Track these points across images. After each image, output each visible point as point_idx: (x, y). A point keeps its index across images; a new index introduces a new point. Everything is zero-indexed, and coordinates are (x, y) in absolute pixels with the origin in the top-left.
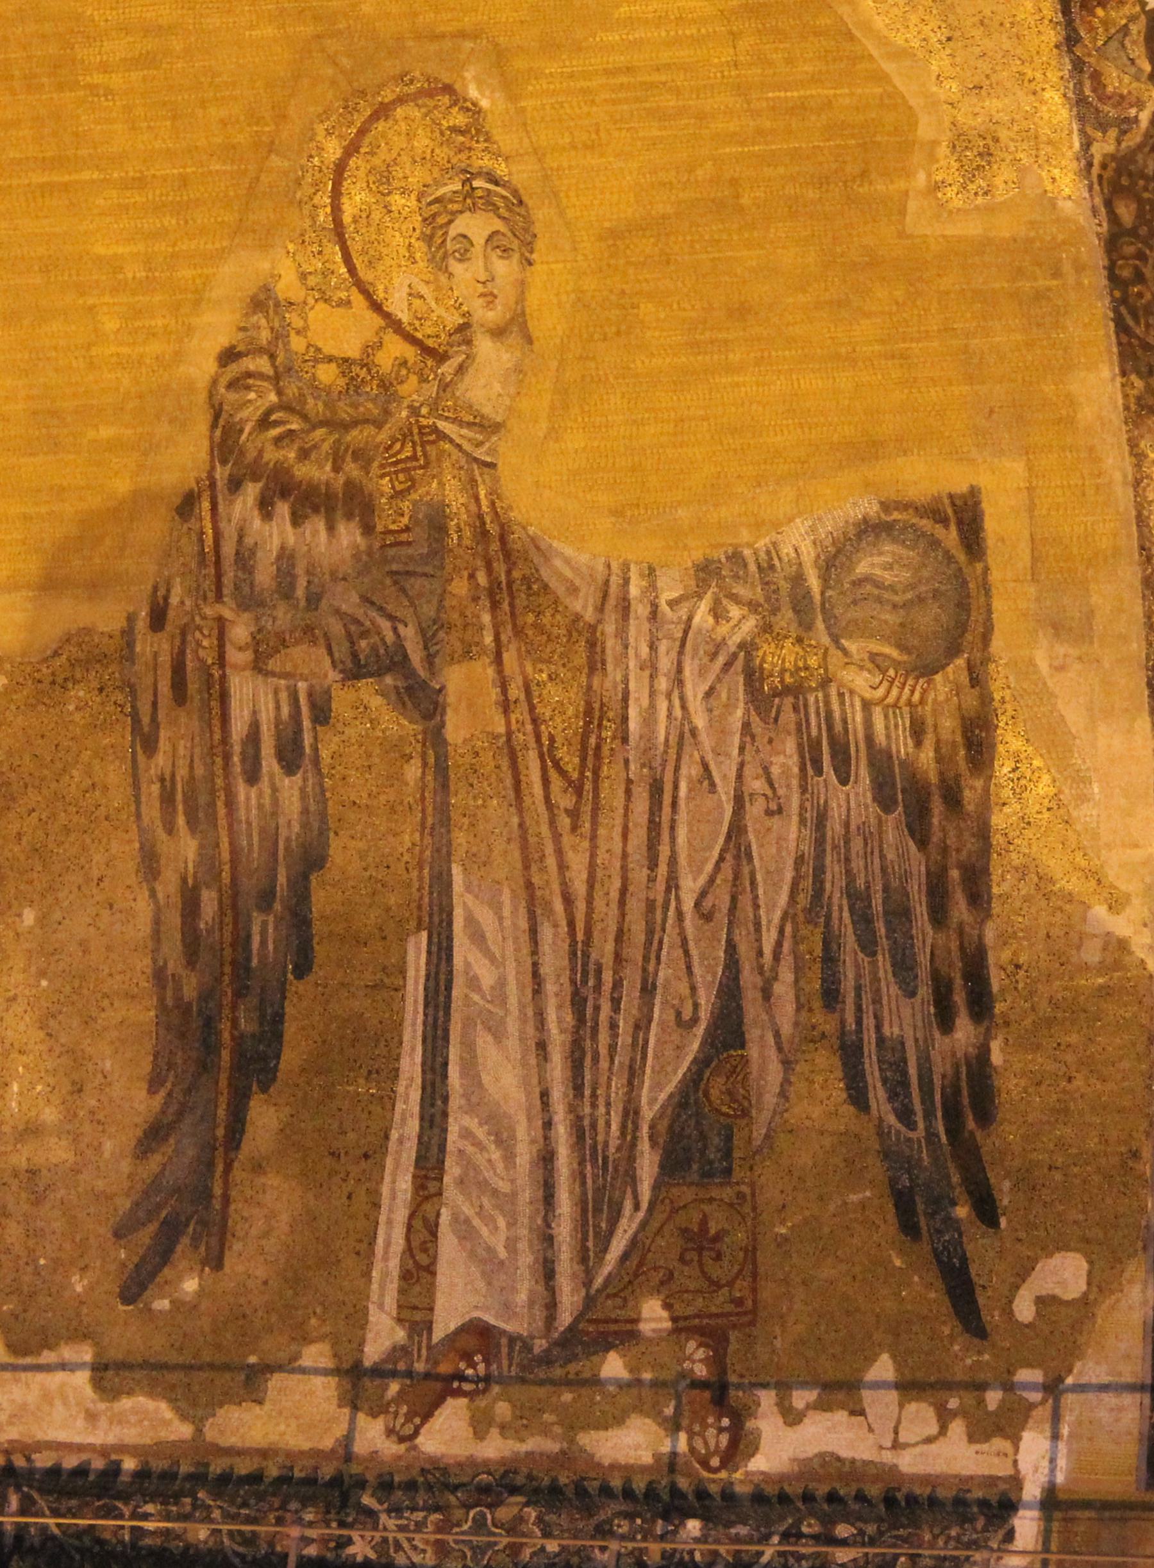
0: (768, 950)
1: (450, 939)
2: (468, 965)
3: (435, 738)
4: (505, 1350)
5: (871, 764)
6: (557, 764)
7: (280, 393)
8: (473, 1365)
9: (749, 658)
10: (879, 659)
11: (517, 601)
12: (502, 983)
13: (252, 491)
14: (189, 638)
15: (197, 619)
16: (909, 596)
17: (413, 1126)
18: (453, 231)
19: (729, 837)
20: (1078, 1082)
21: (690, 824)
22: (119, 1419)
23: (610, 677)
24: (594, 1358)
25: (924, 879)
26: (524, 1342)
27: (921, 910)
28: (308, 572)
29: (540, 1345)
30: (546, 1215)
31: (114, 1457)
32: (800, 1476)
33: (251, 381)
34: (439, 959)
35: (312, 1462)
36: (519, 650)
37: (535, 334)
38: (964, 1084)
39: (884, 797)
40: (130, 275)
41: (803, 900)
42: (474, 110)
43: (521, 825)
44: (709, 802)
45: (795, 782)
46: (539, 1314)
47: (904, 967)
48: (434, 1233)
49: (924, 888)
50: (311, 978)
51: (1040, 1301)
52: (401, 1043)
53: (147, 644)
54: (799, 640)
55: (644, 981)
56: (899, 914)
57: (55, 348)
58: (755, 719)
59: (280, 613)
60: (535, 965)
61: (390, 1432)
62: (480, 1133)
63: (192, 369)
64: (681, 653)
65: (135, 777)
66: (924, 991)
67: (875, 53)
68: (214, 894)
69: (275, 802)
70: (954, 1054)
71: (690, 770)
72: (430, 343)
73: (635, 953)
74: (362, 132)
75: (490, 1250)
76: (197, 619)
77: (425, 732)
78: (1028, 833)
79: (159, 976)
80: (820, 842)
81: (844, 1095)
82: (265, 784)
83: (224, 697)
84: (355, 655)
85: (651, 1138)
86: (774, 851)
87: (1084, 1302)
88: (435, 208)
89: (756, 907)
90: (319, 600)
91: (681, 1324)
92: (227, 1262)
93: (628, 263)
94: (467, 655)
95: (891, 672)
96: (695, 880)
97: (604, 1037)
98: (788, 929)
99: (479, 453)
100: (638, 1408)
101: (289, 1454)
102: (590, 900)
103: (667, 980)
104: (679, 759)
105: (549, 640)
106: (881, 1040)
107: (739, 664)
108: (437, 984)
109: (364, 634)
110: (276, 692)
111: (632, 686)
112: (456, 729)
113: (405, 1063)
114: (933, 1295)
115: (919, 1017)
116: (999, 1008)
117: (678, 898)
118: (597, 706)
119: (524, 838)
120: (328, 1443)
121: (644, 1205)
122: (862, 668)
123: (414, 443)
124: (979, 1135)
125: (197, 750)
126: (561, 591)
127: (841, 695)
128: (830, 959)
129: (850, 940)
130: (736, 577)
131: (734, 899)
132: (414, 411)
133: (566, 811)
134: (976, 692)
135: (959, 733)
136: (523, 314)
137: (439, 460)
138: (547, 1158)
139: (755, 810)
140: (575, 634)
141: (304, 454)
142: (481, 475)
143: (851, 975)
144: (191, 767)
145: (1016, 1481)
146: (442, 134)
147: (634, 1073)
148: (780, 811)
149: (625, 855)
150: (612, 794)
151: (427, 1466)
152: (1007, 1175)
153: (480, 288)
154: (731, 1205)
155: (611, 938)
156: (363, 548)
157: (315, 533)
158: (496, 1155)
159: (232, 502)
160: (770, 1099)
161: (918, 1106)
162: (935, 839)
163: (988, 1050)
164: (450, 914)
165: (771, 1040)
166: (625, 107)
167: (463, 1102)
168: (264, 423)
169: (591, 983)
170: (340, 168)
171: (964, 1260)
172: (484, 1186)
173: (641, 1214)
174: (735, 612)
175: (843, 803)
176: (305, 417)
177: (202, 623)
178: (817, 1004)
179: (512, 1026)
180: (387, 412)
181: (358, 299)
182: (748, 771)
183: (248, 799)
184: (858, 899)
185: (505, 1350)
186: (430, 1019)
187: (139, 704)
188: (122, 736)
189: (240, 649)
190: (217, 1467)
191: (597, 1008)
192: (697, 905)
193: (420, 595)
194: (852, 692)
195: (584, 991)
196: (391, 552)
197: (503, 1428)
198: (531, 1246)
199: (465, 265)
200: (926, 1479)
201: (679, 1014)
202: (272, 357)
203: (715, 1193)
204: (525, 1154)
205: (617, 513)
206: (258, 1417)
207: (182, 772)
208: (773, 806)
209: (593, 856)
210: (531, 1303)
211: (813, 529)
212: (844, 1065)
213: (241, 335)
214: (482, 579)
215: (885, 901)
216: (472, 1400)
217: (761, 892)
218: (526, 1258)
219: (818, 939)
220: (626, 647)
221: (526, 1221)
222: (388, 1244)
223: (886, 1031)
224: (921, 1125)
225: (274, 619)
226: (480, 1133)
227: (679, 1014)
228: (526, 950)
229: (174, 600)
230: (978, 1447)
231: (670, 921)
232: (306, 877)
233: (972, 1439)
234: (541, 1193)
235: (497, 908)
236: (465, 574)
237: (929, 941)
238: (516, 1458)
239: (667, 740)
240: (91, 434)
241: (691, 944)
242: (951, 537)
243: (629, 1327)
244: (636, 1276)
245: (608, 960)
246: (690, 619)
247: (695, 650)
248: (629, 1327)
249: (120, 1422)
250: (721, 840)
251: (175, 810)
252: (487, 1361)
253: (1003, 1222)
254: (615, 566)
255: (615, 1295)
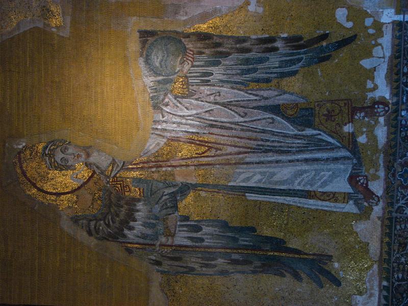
0: (255, 98)
1: (248, 187)
2: (255, 182)
3: (194, 187)
4: (356, 171)
5: (208, 66)
6: (203, 153)
7: (101, 220)
8: (360, 180)
9: (178, 97)
10: (181, 62)
11: (160, 160)
12: (260, 173)
13: (126, 232)
14: (164, 255)
15: (159, 252)
16: (165, 52)
17: (296, 199)
18: (60, 163)
19: (225, 107)
20: (292, 13)
21: (221, 117)
22: (372, 288)
23: (181, 136)
24: (359, 145)
25: (239, 54)
26: (355, 165)
27: (247, 55)
28: (149, 219)
29: (355, 161)
30: (321, 161)
31: (382, 288)
32: (391, 84)
33: (97, 228)
34: (253, 190)
35: (384, 227)
36: (173, 160)
37: (89, 144)
38: (292, 44)
39: (217, 64)
40: (65, 257)
41: (243, 87)
42: (26, 148)
43: (219, 165)
44: (215, 111)
45: (212, 88)
46: (346, 162)
47: (261, 61)
48: (324, 193)
49: (241, 54)
50: (256, 227)
51: (348, 20)
52: (274, 202)
53: (165, 267)
54: (175, 83)
55: (262, 132)
56: (247, 61)
57: (84, 282)
58: (194, 97)
59: (159, 228)
60: (256, 163)
61: (377, 204)
62: (299, 180)
63: (92, 244)
64: (176, 115)
65: (200, 275)
66: (268, 55)
67: (17, 33)
68: (233, 255)
69: (209, 234)
70: (283, 47)
71: (207, 116)
72: (90, 175)
73: (254, 135)
74: (30, 181)
75: (330, 176)
76: (159, 252)
77: (193, 189)
78: (229, 25)
79: (254, 272)
80: (228, 82)
81: (293, 77)
82: (204, 237)
83: (181, 246)
84: (171, 207)
85: (302, 131)
86: (229, 95)
87: (348, 8)
88: (53, 166)
89: (244, 101)
90: (156, 216)
91: (350, 120)
92: (330, 254)
93: (72, 116)
94: (173, 175)
95: (185, 59)
96: (236, 117)
97: (276, 144)
98: (250, 92)
99: (120, 166)
100: (372, 132)
101: (382, 234)
102: (240, 147)
103: (262, 126)
104: (204, 119)
105: (170, 152)
106: (280, 67)
107: (180, 100)
108: (260, 191)
109: (166, 204)
110: (180, 231)
111: (184, 130)
112: (192, 180)
113: (280, 201)
114: (345, 50)
115: (274, 57)
116: (273, 35)
117: (241, 122)
118: (189, 140)
119: (222, 164)
120: (379, 223)
121: (319, 132)
122: (183, 67)
123: (117, 184)
124: (305, 40)
125: (194, 255)
126: (158, 147)
127: (190, 73)
128: (258, 81)
129: (254, 75)
130: (158, 99)
131: (241, 107)
132: (108, 182)
133: (216, 152)
134: (191, 36)
135: (201, 42)
136: (84, 147)
137: (120, 177)
138: (306, 161)
139: (218, 99)
140: (170, 144)
141: (118, 215)
142: (126, 166)
143: (263, 75)
144: (199, 258)
145: (394, 22)
146: (32, 158)
147: (286, 136)
148: (219, 92)
149: (228, 136)
150: (212, 138)
151: (386, 192)
152: (316, 32)
153: (76, 158)
154: (320, 108)
155: (249, 141)
156: (143, 202)
157: (139, 215)
158: (305, 175)
159: (129, 238)
160: (293, 97)
161: (297, 57)
162: (229, 50)
163: (283, 38)
164: (242, 186)
165: (277, 98)
166: (29, 106)
167: (291, 185)
168: (108, 226)
169: (261, 148)
170: (40, 190)
171: (336, 42)
172: (313, 179)
173: (321, 133)
174: (167, 100)
175: (218, 75)
176: (108, 214)
177: (161, 251)
178: (270, 84)
179: (271, 170)
180: (107, 191)
181: (76, 193)
182: (208, 100)
183: (208, 242)
184: (244, 72)
185: (356, 171)
186: (269, 193)
187: (181, 271)
188: (190, 277)
189: (168, 240)
190: (385, 256)
191: (268, 146)
192: (242, 117)
193: (157, 187)
194: (189, 70)
195: (263, 150)
196: (145, 195)
197: (377, 171)
198: (328, 165)
199: (69, 160)
200: (393, 48)
201: (271, 123)
202: (91, 220)
203: (317, 112)
204: (305, 167)
205: (138, 130)
206: (372, 244)
207: (200, 260)
208: (218, 94)
209: (228, 145)
210: (344, 164)
211: (146, 76)
212: (285, 77)
213: (84, 228)
214: (154, 170)
215: (244, 65)
216: (369, 180)
217: (240, 99)
218: (332, 166)
219: (253, 84)
220: (174, 130)
221: (322, 166)
222: (327, 206)
223: (277, 65)
224: (302, 56)
225: (161, 229)
226: (299, 180)
227: (271, 123)
228: (252, 166)
229: (154, 258)
230: (384, 34)
231: (247, 125)
232: (230, 227)
233: (383, 36)
234: (316, 162)
235: (240, 173)
236: (152, 174)
237: (255, 53)
238: (384, 166)
239: (199, 122)
240: (108, 276)
241: (252, 119)
242: (151, 40)
243: (351, 136)
244: (337, 134)
245: (255, 143)
246: (167, 112)
247: (175, 111)
248: (351, 136)
249: (373, 286)
250: (226, 109)
251: (210, 264)
252: (358, 177)
253: (328, 32)
254: (152, 132)
255: (342, 139)
